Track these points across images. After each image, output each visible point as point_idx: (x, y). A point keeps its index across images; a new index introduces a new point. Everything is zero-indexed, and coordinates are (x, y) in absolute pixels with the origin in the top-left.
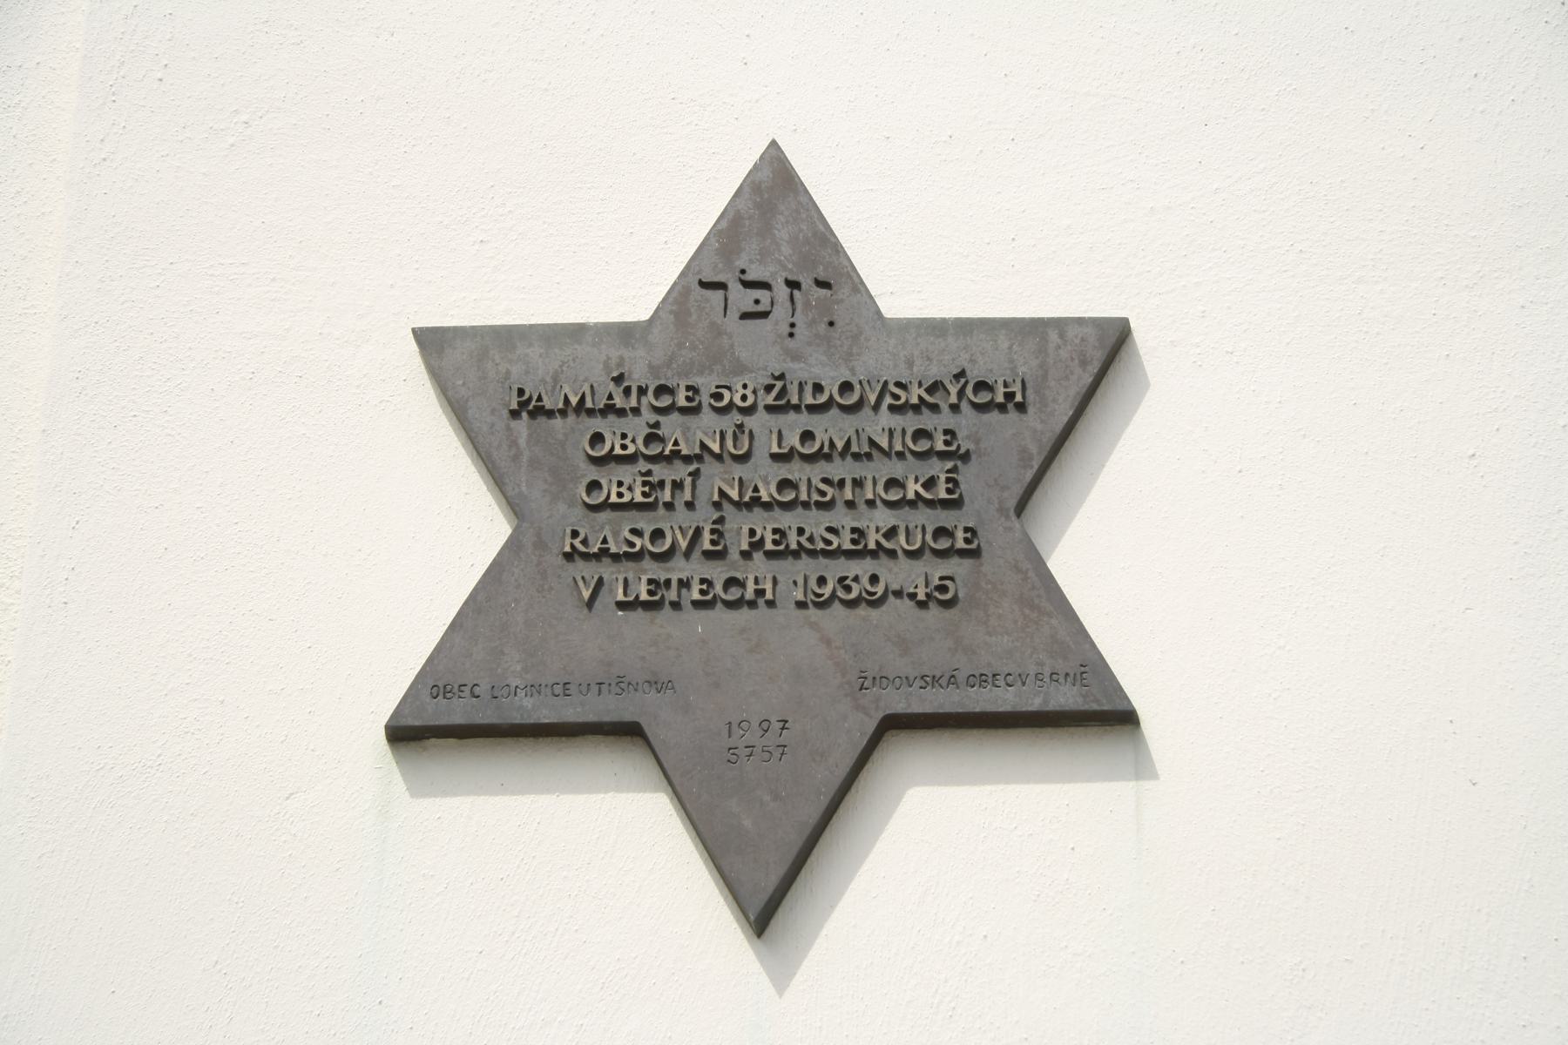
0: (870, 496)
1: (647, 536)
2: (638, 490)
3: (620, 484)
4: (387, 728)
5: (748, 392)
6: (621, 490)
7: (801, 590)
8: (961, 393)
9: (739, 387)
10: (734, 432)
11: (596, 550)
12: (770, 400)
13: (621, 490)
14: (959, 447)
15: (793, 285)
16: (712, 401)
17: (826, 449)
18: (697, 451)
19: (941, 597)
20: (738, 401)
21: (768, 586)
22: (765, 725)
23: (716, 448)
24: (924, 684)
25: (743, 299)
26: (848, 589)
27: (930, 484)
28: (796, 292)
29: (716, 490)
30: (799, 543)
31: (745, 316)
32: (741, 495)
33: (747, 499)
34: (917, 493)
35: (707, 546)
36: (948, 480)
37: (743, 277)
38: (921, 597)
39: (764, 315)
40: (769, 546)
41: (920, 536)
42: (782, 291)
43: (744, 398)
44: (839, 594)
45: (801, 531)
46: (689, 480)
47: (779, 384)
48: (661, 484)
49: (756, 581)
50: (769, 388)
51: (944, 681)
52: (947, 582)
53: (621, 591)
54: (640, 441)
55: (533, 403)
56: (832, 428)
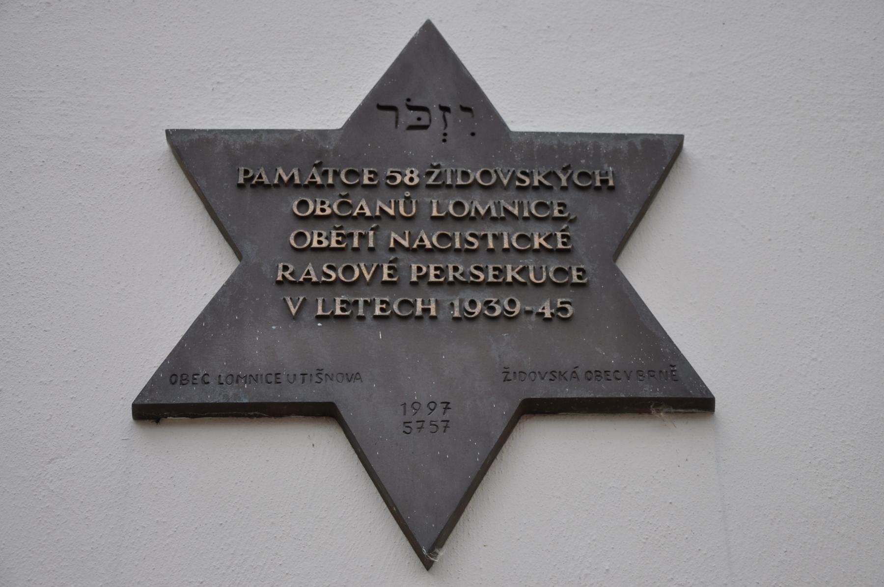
0: (506, 246)
1: (340, 271)
2: (334, 239)
3: (320, 235)
4: (132, 404)
5: (414, 176)
6: (320, 239)
7: (457, 309)
8: (569, 179)
9: (408, 172)
10: (405, 202)
11: (301, 280)
12: (430, 181)
13: (320, 239)
14: (569, 214)
15: (445, 109)
16: (388, 181)
17: (473, 214)
18: (378, 213)
19: (560, 317)
20: (407, 181)
21: (433, 307)
22: (432, 406)
23: (391, 212)
24: (552, 378)
25: (411, 117)
26: (493, 309)
27: (550, 238)
28: (447, 114)
29: (392, 240)
30: (454, 277)
31: (411, 128)
32: (411, 243)
33: (415, 246)
34: (540, 244)
35: (385, 278)
36: (563, 236)
37: (410, 104)
38: (548, 315)
39: (425, 127)
40: (432, 279)
41: (544, 274)
42: (437, 115)
43: (411, 179)
44: (486, 312)
45: (456, 269)
46: (371, 233)
47: (437, 171)
48: (351, 235)
49: (423, 303)
50: (430, 174)
51: (568, 375)
52: (567, 306)
53: (320, 308)
54: (335, 207)
55: (255, 180)
56: (476, 204)
